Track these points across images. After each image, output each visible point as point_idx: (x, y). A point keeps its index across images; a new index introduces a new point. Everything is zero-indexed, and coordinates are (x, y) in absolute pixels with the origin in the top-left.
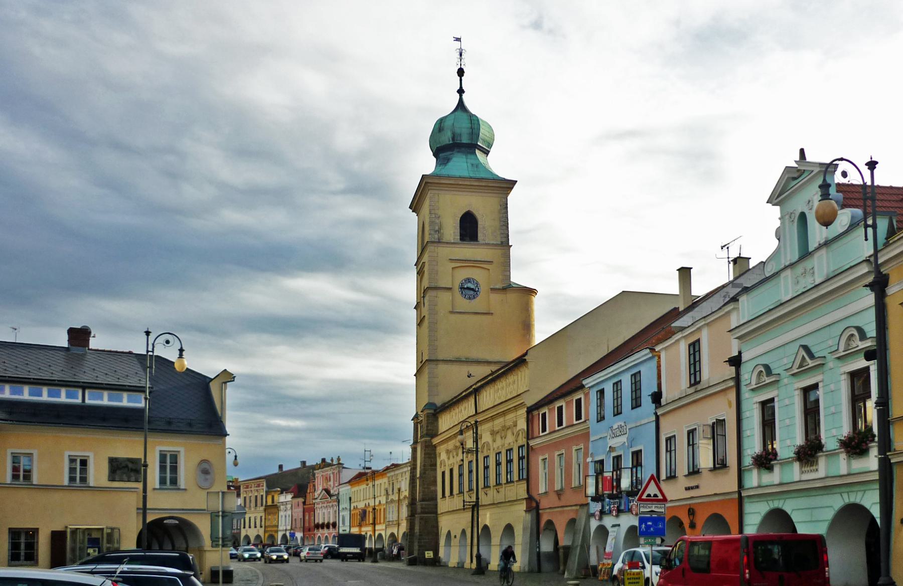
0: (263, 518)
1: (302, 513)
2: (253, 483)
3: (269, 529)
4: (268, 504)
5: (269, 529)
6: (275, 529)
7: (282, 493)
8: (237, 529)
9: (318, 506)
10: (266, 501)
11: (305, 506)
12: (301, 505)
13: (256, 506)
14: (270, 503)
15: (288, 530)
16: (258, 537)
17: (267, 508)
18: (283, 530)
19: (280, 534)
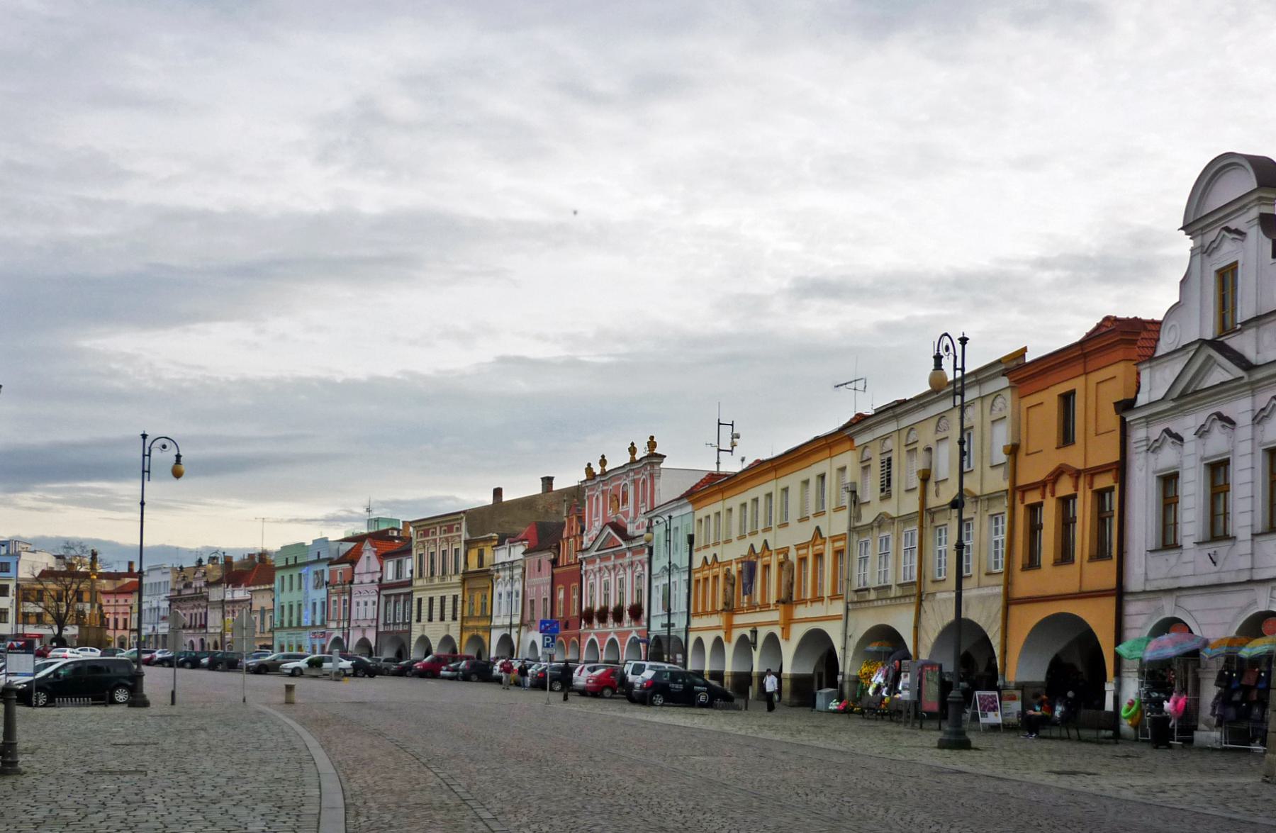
0: (460, 599)
1: (549, 587)
2: (439, 523)
3: (471, 624)
4: (470, 570)
5: (471, 624)
6: (484, 623)
7: (501, 542)
8: (404, 623)
9: (590, 567)
10: (466, 563)
11: (555, 571)
12: (547, 567)
13: (444, 573)
14: (473, 566)
15: (516, 626)
16: (447, 640)
17: (467, 577)
18: (503, 627)
19: (496, 636)
